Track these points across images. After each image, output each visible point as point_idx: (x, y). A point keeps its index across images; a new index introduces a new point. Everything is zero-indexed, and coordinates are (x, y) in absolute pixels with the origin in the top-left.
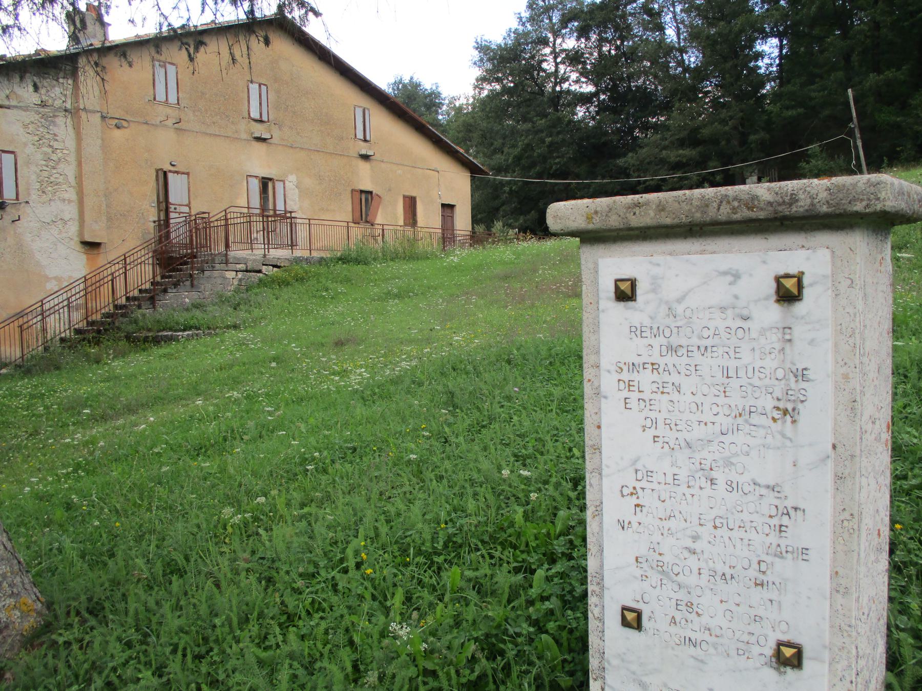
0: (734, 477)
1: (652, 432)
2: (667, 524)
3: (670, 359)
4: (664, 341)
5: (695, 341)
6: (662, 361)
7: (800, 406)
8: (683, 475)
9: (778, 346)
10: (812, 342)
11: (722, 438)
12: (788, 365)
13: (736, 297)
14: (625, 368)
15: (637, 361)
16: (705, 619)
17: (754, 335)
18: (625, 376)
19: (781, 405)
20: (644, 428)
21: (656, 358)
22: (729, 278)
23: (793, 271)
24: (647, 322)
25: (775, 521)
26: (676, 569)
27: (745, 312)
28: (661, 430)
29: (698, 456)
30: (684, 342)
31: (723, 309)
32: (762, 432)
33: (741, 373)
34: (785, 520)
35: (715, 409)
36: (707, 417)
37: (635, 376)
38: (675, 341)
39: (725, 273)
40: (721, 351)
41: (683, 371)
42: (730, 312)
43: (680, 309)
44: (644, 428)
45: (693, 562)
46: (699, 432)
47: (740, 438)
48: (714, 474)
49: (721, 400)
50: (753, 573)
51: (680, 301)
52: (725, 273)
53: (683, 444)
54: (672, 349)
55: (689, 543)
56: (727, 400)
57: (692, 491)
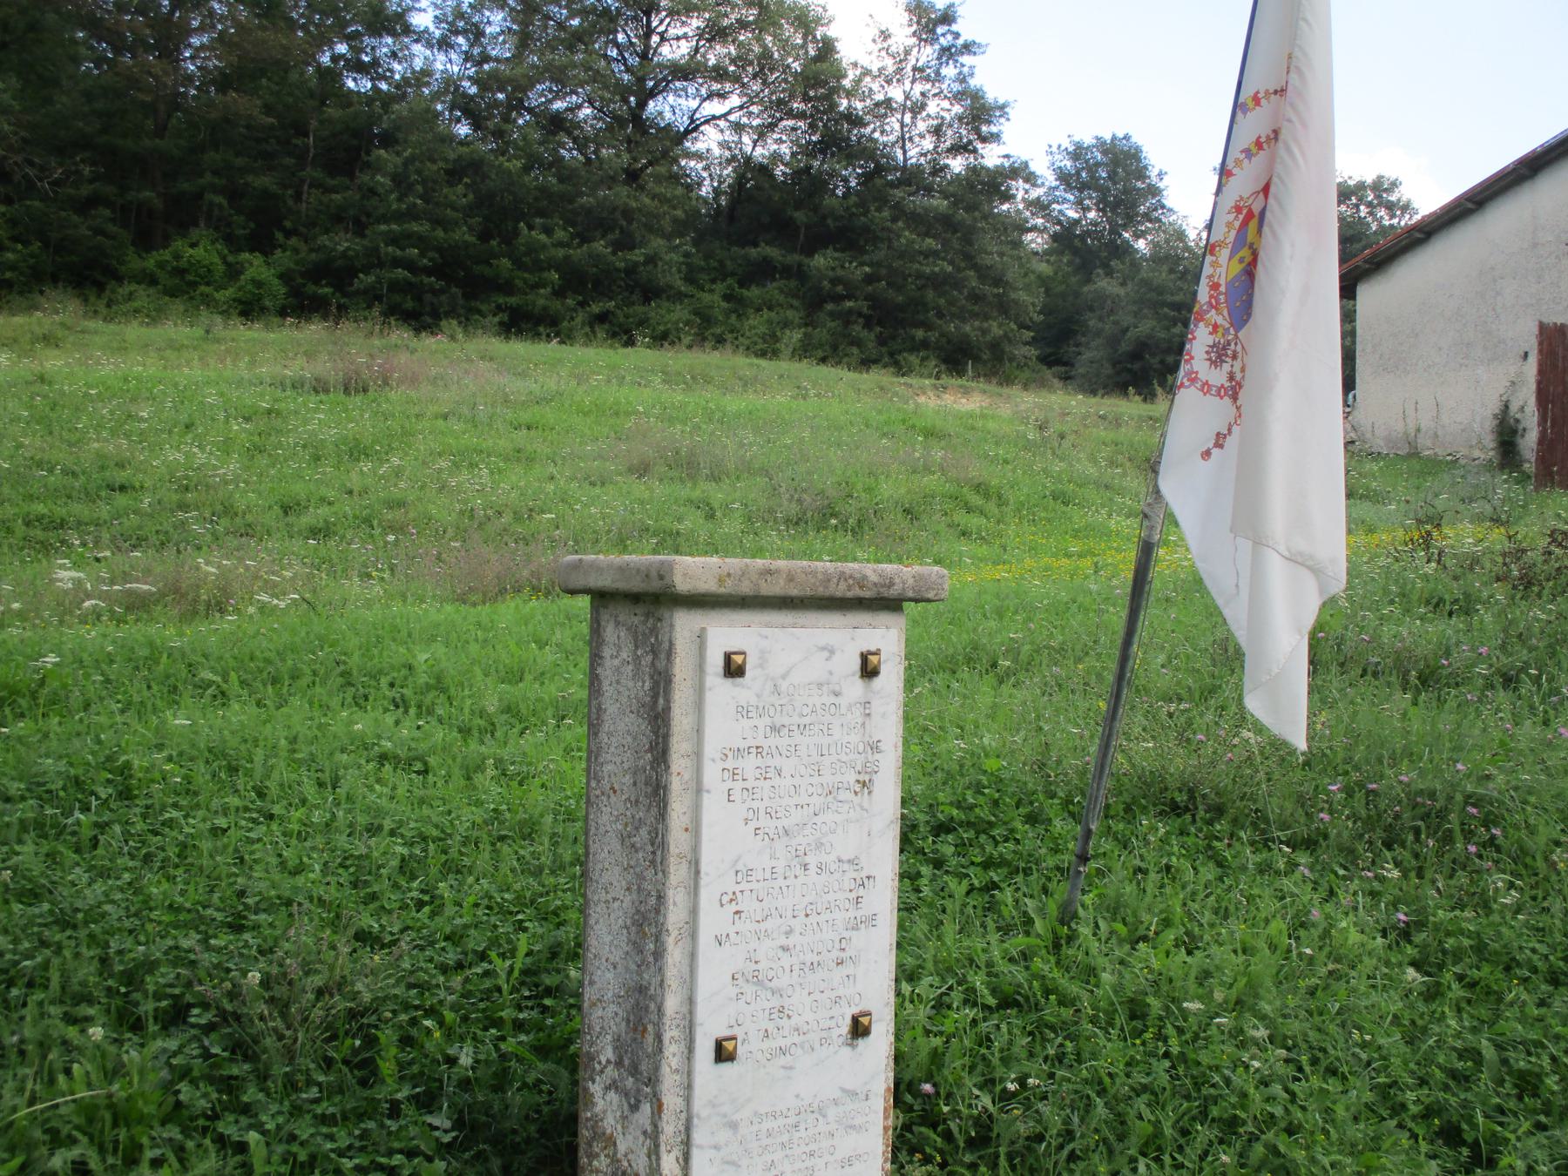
0: (824, 858)
1: (752, 825)
2: (763, 926)
3: (773, 741)
4: (768, 721)
5: (796, 720)
6: (765, 744)
7: (874, 777)
8: (780, 865)
9: (860, 720)
10: (884, 715)
11: (816, 819)
12: (867, 739)
13: (831, 673)
14: (730, 755)
15: (743, 745)
16: (795, 1020)
17: (843, 711)
18: (730, 764)
19: (861, 778)
20: (746, 821)
21: (760, 741)
22: (826, 654)
23: (873, 649)
24: (754, 701)
25: (853, 895)
26: (771, 974)
27: (837, 688)
28: (764, 822)
29: (794, 842)
30: (786, 721)
31: (820, 685)
32: (846, 807)
33: (833, 750)
34: (861, 892)
35: (811, 790)
36: (804, 799)
37: (740, 763)
38: (778, 721)
39: (823, 649)
40: (816, 728)
41: (784, 752)
42: (825, 688)
43: (784, 685)
44: (746, 821)
45: (786, 960)
46: (797, 816)
47: (828, 817)
48: (807, 859)
49: (816, 780)
50: (836, 954)
51: (784, 677)
52: (823, 649)
53: (781, 832)
54: (775, 729)
55: (783, 941)
56: (820, 780)
57: (788, 882)
